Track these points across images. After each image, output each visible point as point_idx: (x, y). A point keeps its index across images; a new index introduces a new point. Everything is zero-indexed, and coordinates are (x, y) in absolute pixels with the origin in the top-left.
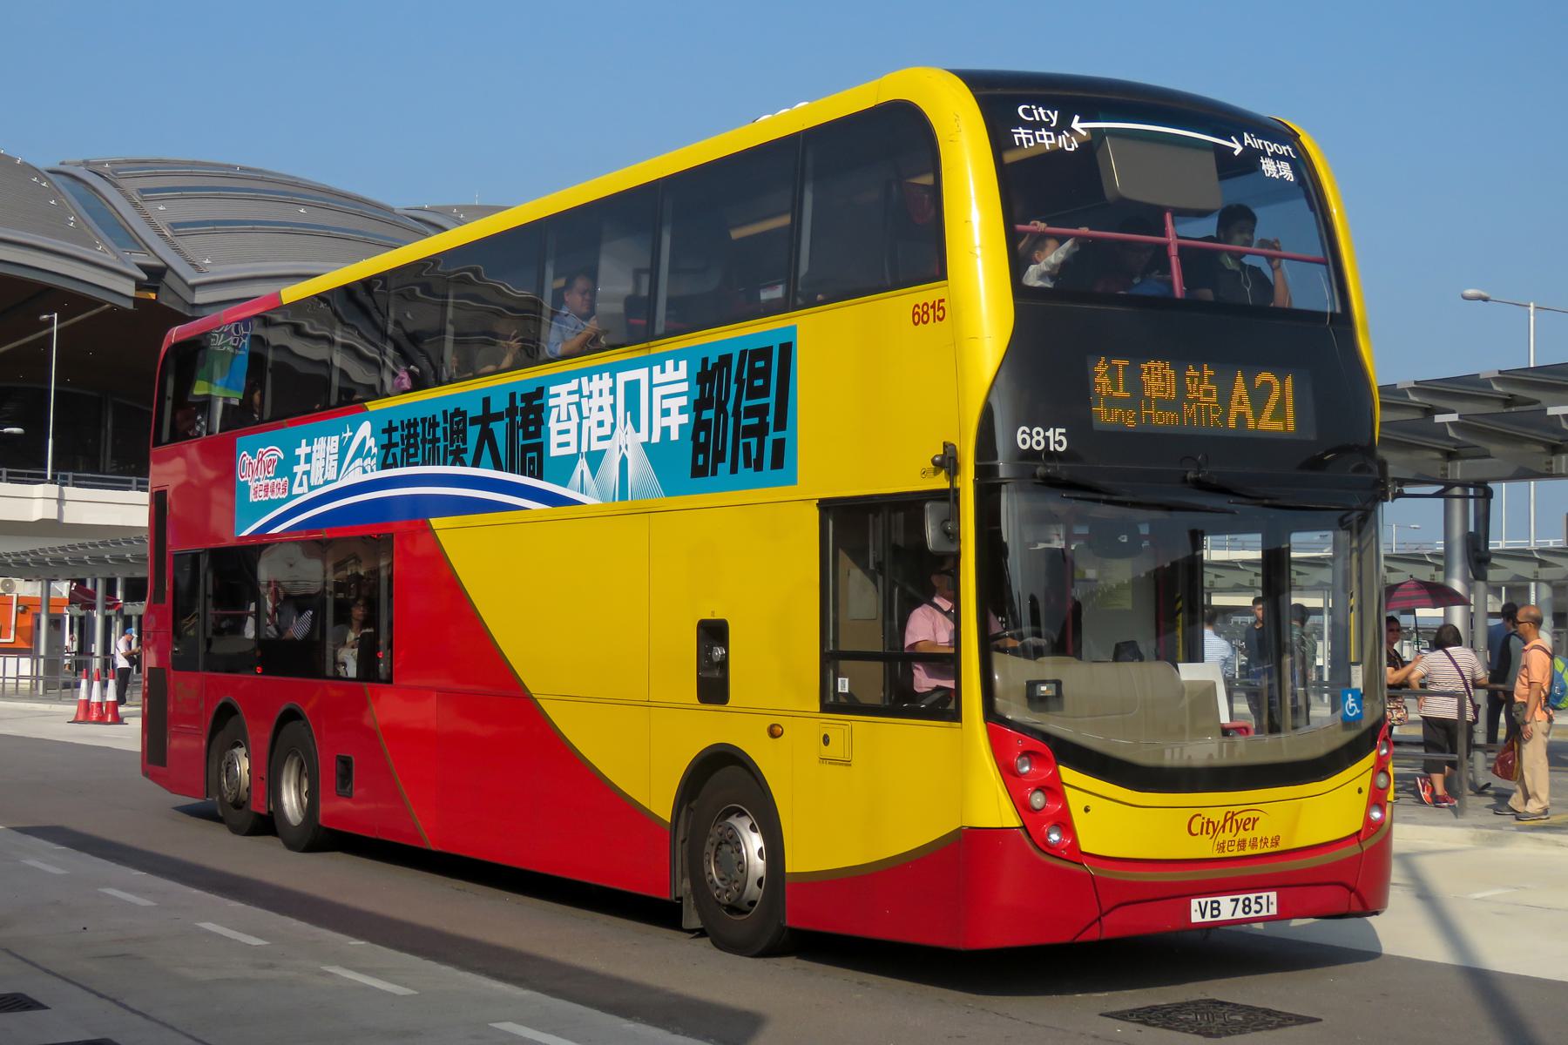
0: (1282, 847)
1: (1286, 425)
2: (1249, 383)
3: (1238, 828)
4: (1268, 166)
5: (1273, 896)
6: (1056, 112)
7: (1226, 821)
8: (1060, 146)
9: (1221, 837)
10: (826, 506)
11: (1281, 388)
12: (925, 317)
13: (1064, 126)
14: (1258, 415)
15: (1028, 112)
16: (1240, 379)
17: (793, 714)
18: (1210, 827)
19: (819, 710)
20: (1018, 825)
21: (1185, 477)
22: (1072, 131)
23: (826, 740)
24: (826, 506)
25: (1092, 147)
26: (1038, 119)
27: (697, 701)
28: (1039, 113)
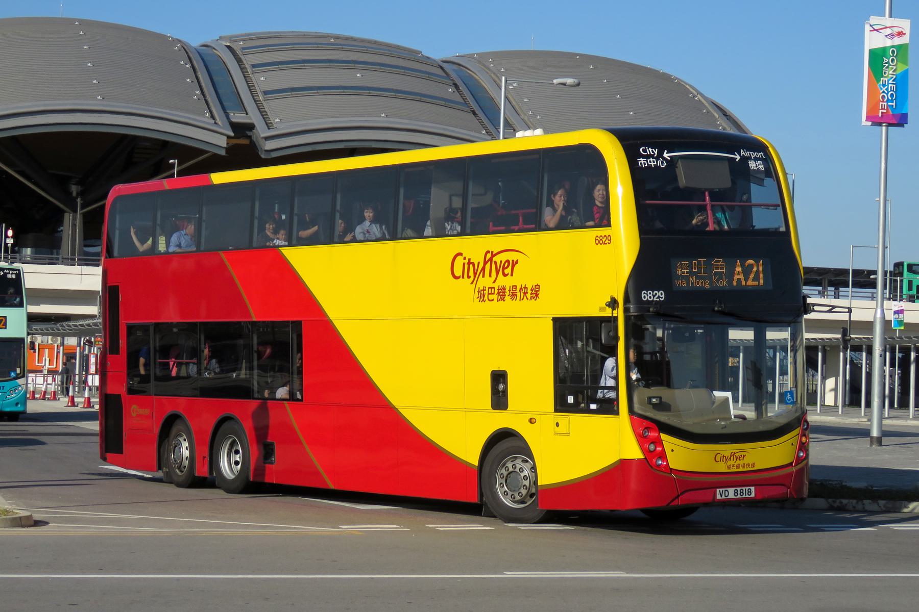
0: (756, 468)
1: (759, 283)
2: (743, 265)
3: (736, 460)
4: (752, 165)
5: (753, 489)
6: (657, 150)
7: (731, 456)
8: (659, 165)
9: (729, 463)
10: (555, 320)
11: (757, 266)
12: (601, 241)
13: (660, 155)
14: (746, 280)
15: (645, 151)
16: (738, 264)
17: (541, 413)
18: (725, 459)
19: (553, 411)
20: (641, 456)
21: (713, 310)
22: (664, 159)
23: (557, 425)
24: (555, 320)
25: (672, 162)
26: (649, 153)
27: (491, 409)
28: (649, 151)
